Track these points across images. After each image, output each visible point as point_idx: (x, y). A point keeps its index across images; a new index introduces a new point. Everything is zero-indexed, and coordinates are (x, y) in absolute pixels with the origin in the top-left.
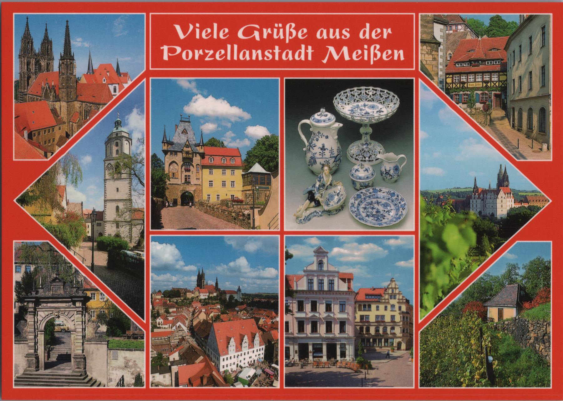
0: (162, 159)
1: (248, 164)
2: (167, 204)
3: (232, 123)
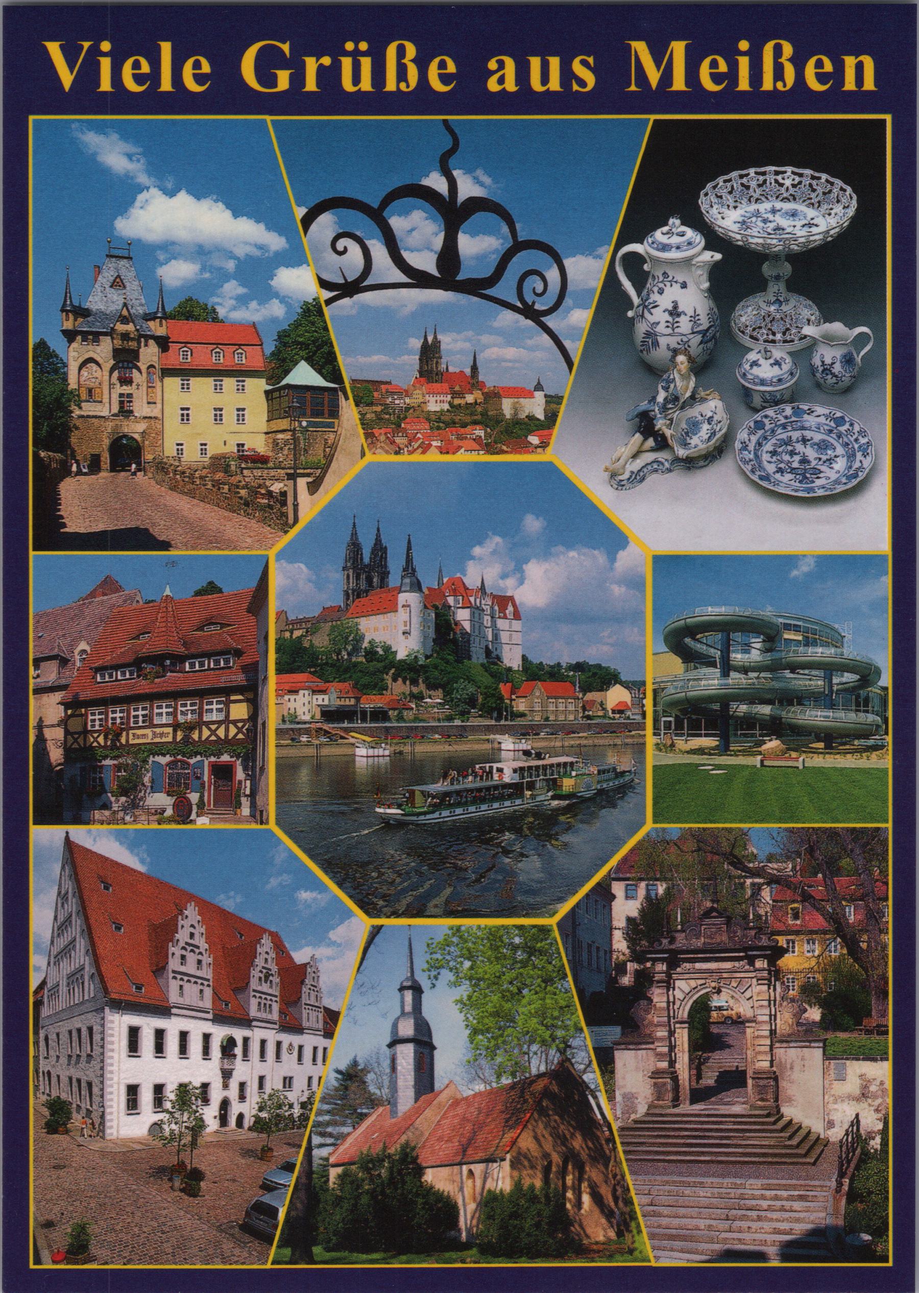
1: (280, 364)
2: (74, 468)
3: (238, 259)
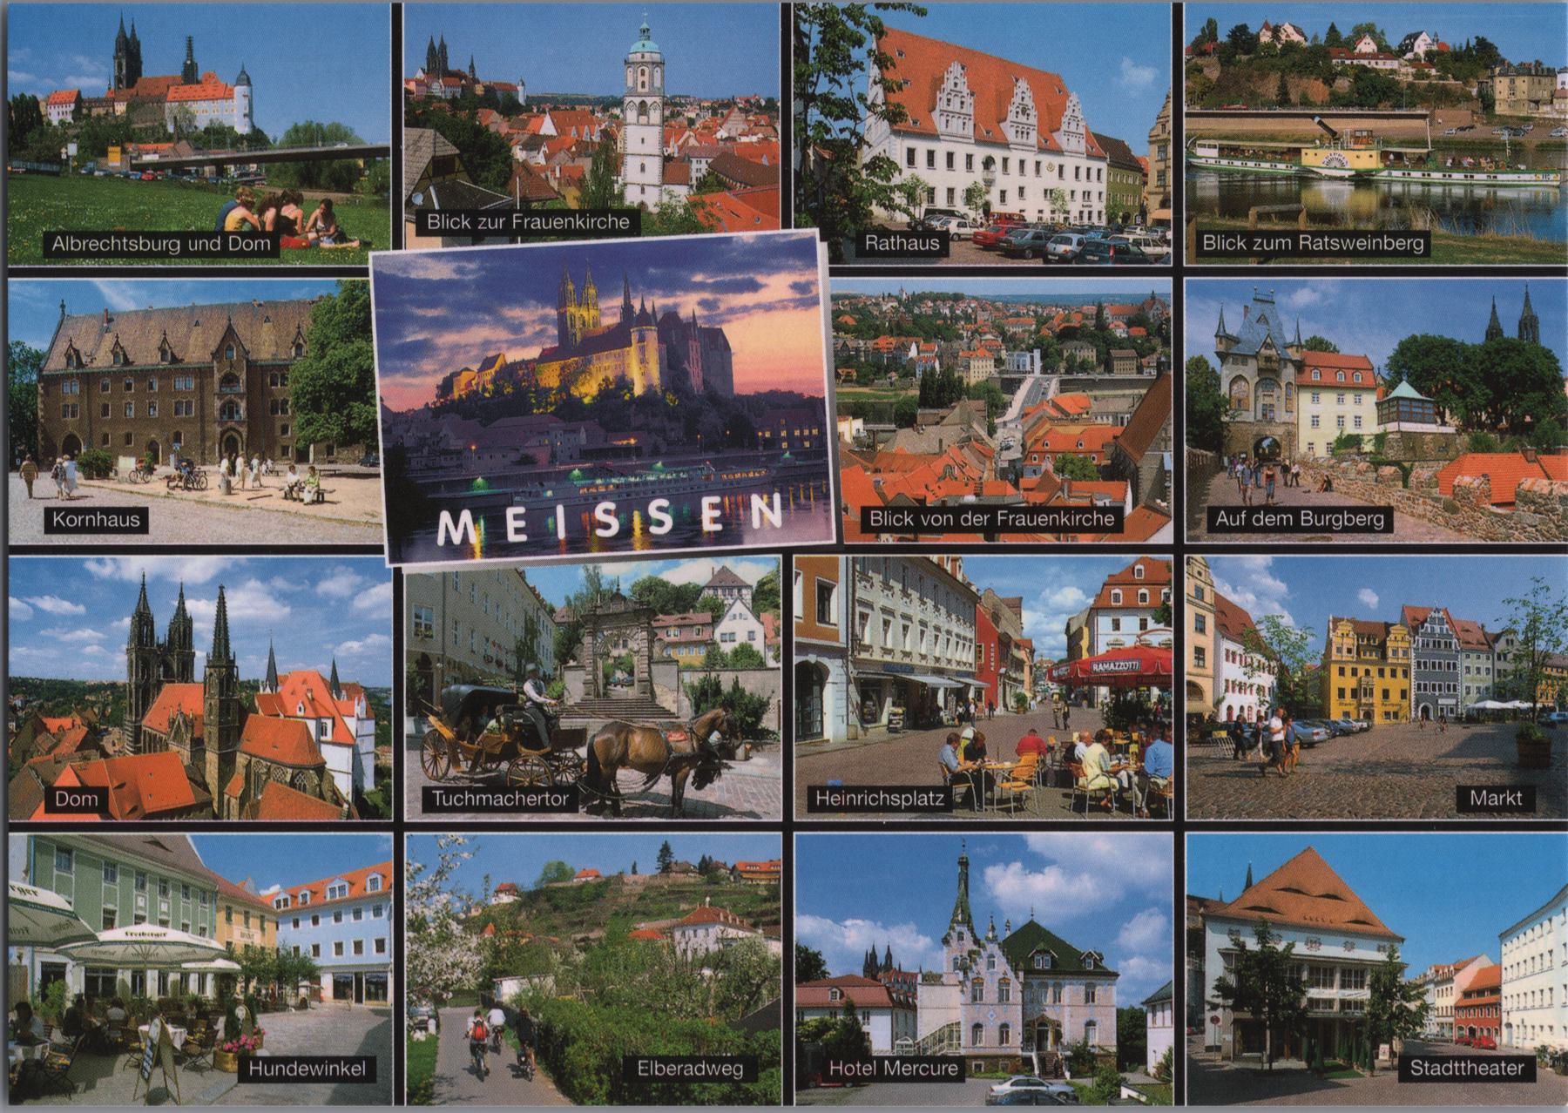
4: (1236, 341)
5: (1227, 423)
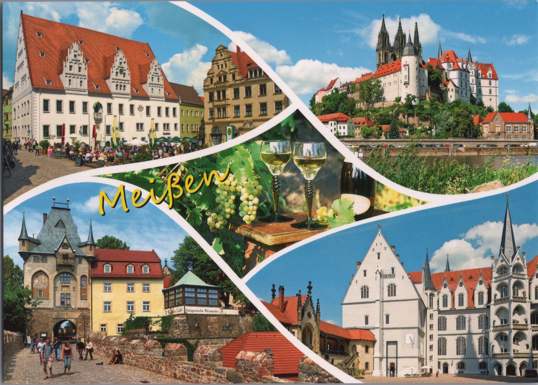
0: (22, 268)
4: (36, 243)
5: (30, 310)
